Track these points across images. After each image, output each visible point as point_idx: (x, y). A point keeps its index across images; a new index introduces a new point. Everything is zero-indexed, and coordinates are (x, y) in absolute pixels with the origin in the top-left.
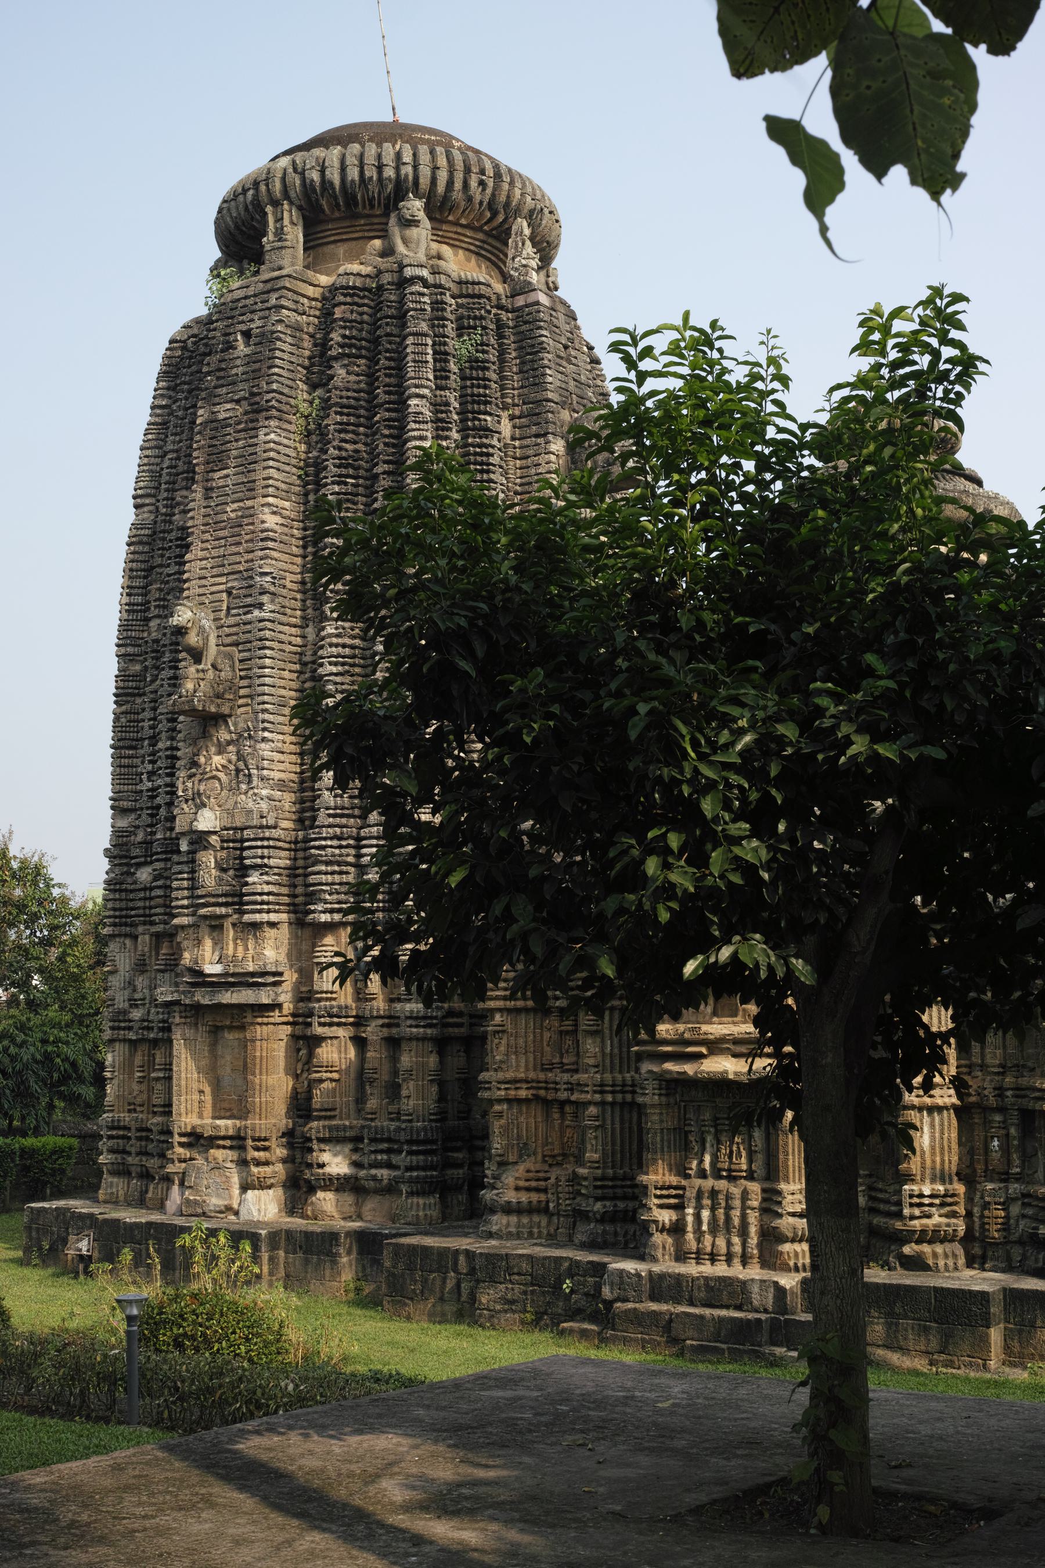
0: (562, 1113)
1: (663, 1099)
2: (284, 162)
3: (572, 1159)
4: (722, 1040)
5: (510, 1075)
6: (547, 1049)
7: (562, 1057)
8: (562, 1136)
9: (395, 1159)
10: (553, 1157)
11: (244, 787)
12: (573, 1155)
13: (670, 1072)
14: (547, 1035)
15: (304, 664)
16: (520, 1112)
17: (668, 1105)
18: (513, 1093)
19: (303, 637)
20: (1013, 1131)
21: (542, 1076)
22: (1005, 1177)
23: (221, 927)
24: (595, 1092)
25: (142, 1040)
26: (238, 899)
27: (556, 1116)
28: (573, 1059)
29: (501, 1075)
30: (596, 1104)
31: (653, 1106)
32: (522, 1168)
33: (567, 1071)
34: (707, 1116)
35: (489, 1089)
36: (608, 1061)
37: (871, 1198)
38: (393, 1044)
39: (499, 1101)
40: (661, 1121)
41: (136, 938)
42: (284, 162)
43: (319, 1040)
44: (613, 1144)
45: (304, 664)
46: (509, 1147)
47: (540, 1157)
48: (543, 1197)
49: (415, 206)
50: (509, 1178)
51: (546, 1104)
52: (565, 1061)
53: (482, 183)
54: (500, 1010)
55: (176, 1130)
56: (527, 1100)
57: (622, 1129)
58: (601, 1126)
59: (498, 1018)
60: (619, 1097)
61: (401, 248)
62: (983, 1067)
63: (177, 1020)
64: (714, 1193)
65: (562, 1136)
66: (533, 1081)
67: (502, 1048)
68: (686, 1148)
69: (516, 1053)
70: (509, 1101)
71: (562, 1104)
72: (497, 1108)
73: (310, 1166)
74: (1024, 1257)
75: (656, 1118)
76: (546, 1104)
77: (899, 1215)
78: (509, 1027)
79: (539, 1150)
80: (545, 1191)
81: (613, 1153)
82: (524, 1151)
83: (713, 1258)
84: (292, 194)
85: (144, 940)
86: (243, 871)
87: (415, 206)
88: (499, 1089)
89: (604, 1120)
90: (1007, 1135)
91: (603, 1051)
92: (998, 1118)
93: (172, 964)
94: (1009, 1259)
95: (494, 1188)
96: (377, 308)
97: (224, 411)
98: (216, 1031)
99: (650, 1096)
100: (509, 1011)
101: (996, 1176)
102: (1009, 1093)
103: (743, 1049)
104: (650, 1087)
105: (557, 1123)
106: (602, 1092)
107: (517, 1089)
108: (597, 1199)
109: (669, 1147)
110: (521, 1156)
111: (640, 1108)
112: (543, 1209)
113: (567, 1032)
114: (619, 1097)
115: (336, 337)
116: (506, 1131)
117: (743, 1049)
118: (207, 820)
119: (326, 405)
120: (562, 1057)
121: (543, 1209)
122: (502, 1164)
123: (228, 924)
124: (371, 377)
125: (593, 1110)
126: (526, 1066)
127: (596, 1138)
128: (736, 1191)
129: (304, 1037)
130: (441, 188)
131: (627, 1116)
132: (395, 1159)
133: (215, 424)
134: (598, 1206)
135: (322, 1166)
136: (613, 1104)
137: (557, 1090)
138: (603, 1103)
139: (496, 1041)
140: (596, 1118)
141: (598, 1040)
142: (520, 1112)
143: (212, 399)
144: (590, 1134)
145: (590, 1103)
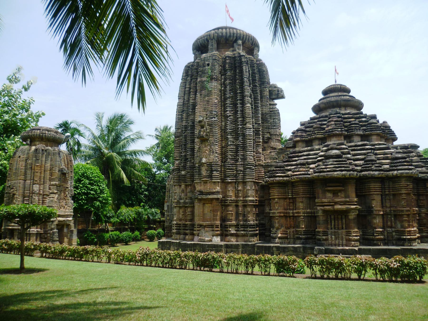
2: (213, 32)
4: (339, 202)
9: (246, 229)
11: (212, 154)
14: (286, 203)
15: (222, 130)
19: (221, 124)
20: (393, 219)
21: (285, 211)
22: (391, 227)
23: (207, 183)
25: (183, 206)
26: (211, 176)
29: (278, 211)
32: (281, 230)
34: (333, 217)
37: (363, 233)
38: (245, 206)
39: (277, 216)
41: (180, 186)
42: (213, 32)
43: (228, 205)
45: (222, 130)
46: (279, 225)
48: (286, 235)
49: (240, 42)
50: (279, 232)
53: (251, 39)
55: (196, 224)
59: (276, 200)
61: (237, 50)
62: (386, 207)
63: (196, 202)
64: (335, 232)
67: (278, 206)
68: (327, 223)
70: (279, 216)
71: (290, 217)
72: (277, 218)
73: (228, 231)
74: (396, 243)
76: (286, 217)
77: (374, 235)
80: (287, 234)
82: (282, 226)
83: (335, 245)
84: (215, 38)
85: (183, 186)
86: (212, 171)
87: (240, 42)
90: (391, 220)
92: (389, 216)
93: (192, 192)
94: (393, 243)
95: (276, 234)
96: (235, 61)
97: (204, 79)
98: (204, 204)
99: (320, 213)
103: (342, 203)
108: (304, 235)
111: (315, 217)
112: (287, 238)
115: (227, 66)
116: (278, 223)
117: (342, 203)
118: (204, 160)
119: (225, 79)
121: (287, 238)
122: (278, 229)
123: (208, 182)
124: (235, 75)
128: (340, 231)
129: (224, 205)
130: (244, 39)
132: (246, 229)
133: (202, 82)
134: (304, 236)
135: (230, 231)
143: (201, 76)
145: (301, 216)
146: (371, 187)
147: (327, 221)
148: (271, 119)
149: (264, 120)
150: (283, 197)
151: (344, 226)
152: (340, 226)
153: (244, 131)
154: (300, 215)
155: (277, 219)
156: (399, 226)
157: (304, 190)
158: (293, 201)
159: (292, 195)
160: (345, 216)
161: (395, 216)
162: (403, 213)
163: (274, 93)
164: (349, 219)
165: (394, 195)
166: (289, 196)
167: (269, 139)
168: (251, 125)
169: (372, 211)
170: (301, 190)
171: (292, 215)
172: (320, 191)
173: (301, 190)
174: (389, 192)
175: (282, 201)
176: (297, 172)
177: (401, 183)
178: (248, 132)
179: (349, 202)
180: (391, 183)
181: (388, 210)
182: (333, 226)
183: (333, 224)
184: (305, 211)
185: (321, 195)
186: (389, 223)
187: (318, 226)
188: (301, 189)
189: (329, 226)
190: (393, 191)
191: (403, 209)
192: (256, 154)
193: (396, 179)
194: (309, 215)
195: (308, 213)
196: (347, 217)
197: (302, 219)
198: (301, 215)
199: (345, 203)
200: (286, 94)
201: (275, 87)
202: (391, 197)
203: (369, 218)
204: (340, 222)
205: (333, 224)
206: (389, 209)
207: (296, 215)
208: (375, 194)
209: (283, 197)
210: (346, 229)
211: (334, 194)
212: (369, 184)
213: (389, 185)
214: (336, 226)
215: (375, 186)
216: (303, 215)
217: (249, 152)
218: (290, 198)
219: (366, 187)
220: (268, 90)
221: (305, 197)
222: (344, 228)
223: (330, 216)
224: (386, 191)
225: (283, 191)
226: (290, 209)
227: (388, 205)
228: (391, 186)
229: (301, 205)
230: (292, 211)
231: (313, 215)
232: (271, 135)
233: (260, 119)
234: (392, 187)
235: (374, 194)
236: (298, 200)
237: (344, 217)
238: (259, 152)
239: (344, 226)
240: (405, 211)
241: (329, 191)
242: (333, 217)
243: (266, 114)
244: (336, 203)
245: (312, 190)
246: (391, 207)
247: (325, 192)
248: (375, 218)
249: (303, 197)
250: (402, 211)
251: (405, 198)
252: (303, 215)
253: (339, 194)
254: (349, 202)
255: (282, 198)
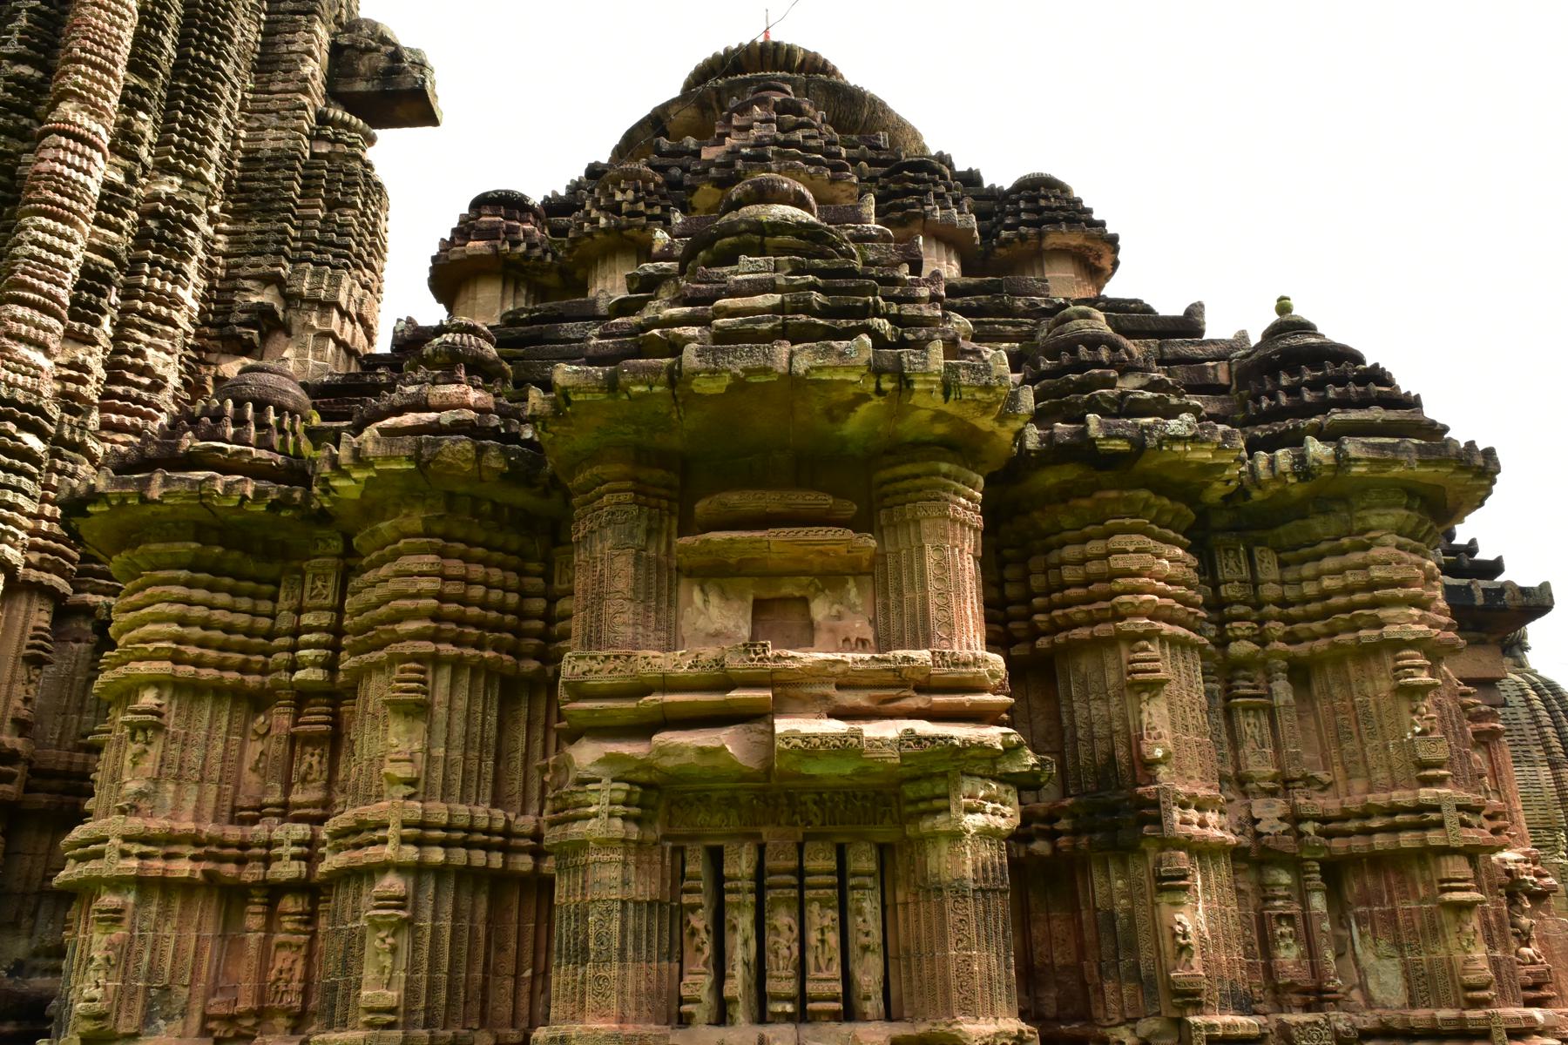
0: (272, 916)
1: (634, 832)
3: (281, 1022)
4: (819, 674)
5: (158, 824)
6: (250, 779)
7: (287, 790)
8: (264, 969)
10: (231, 1019)
12: (286, 1011)
13: (679, 750)
14: (254, 749)
16: (165, 913)
17: (640, 844)
18: (158, 864)
20: (1318, 902)
21: (234, 833)
24: (404, 840)
27: (254, 921)
28: (315, 794)
29: (136, 824)
30: (401, 869)
31: (606, 844)
33: (298, 819)
34: (740, 865)
35: (99, 855)
36: (438, 774)
40: (625, 883)
44: (434, 965)
46: (124, 995)
47: (195, 1020)
51: (232, 897)
52: (296, 797)
54: (157, 683)
56: (187, 887)
57: (455, 932)
58: (408, 922)
59: (148, 699)
60: (459, 856)
65: (264, 969)
66: (211, 840)
67: (149, 765)
68: (676, 953)
69: (178, 779)
70: (142, 884)
71: (274, 892)
72: (109, 900)
75: (614, 873)
76: (232, 897)
78: (172, 723)
79: (197, 1006)
81: (432, 988)
88: (125, 854)
89: (416, 909)
91: (428, 751)
99: (602, 818)
100: (179, 687)
101: (1297, 999)
102: (1309, 827)
103: (859, 699)
104: (603, 798)
105: (253, 939)
106: (419, 842)
107: (168, 857)
109: (637, 949)
110: (148, 1020)
113: (310, 740)
114: (459, 856)
116: (122, 958)
120: (287, 790)
125: (392, 884)
126: (198, 809)
127: (394, 950)
131: (466, 904)
136: (440, 871)
137: (267, 861)
138: (417, 870)
139: (134, 748)
140: (401, 902)
141: (421, 727)
142: (165, 913)
144: (377, 942)
145: (385, 867)
146: (1118, 562)
147: (680, 914)
148: (308, 210)
149: (254, 191)
150: (231, 676)
151: (869, 975)
152: (825, 982)
153: (25, 158)
154: (371, 854)
155: (114, 917)
156: (1387, 983)
157: (452, 588)
158: (328, 718)
159: (331, 666)
160: (884, 852)
161: (1334, 873)
162: (1434, 837)
163: (363, 65)
164: (934, 890)
165: (1300, 673)
166: (293, 667)
167: (270, 324)
168: (97, 113)
169: (1150, 812)
170: (426, 584)
171: (288, 870)
172: (621, 573)
173: (426, 584)
174: (1262, 640)
175: (209, 728)
176: (399, 411)
177: (1376, 552)
178: (50, 153)
179: (926, 686)
180: (1269, 567)
181: (1270, 814)
182: (736, 985)
183: (740, 952)
184: (439, 811)
185: (622, 619)
186: (1288, 955)
187: (561, 976)
188: (408, 578)
189: (699, 983)
190: (1291, 638)
191: (1426, 794)
192: (114, 378)
193: (1317, 525)
194: (479, 858)
195: (467, 835)
196: (898, 863)
197: (383, 901)
198: (388, 852)
199: (889, 691)
200: (444, 97)
201: (384, 40)
202: (1282, 691)
203: (1111, 887)
204: (822, 919)
205: (740, 952)
206: (1279, 806)
207: (332, 862)
208: (1163, 640)
209: (231, 676)
210: (889, 1016)
211: (760, 608)
212: (1094, 547)
213: (1255, 583)
214: (781, 983)
215: (1158, 566)
216: (410, 853)
217: (25, 312)
218: (302, 697)
219: (1068, 574)
220: (322, 33)
221: (457, 664)
222: (873, 1006)
223: (716, 857)
224: (1241, 628)
225: (242, 620)
226: (285, 812)
227: (1260, 766)
228: (1270, 591)
229: (390, 745)
230: (301, 830)
231: (524, 863)
232: (290, 299)
233: (215, 154)
234: (1283, 603)
235: (1149, 635)
236: (377, 690)
237: (863, 861)
238: (145, 370)
239: (869, 975)
240: (1451, 817)
241: (716, 574)
242: (740, 865)
243: (283, 159)
244: (791, 691)
245: (538, 605)
246: (1284, 784)
247: (661, 585)
248: (1172, 885)
249: (436, 660)
250: (1423, 816)
251: (1423, 690)
252: (410, 853)
253: (820, 610)
254: (926, 686)
255: (218, 691)
